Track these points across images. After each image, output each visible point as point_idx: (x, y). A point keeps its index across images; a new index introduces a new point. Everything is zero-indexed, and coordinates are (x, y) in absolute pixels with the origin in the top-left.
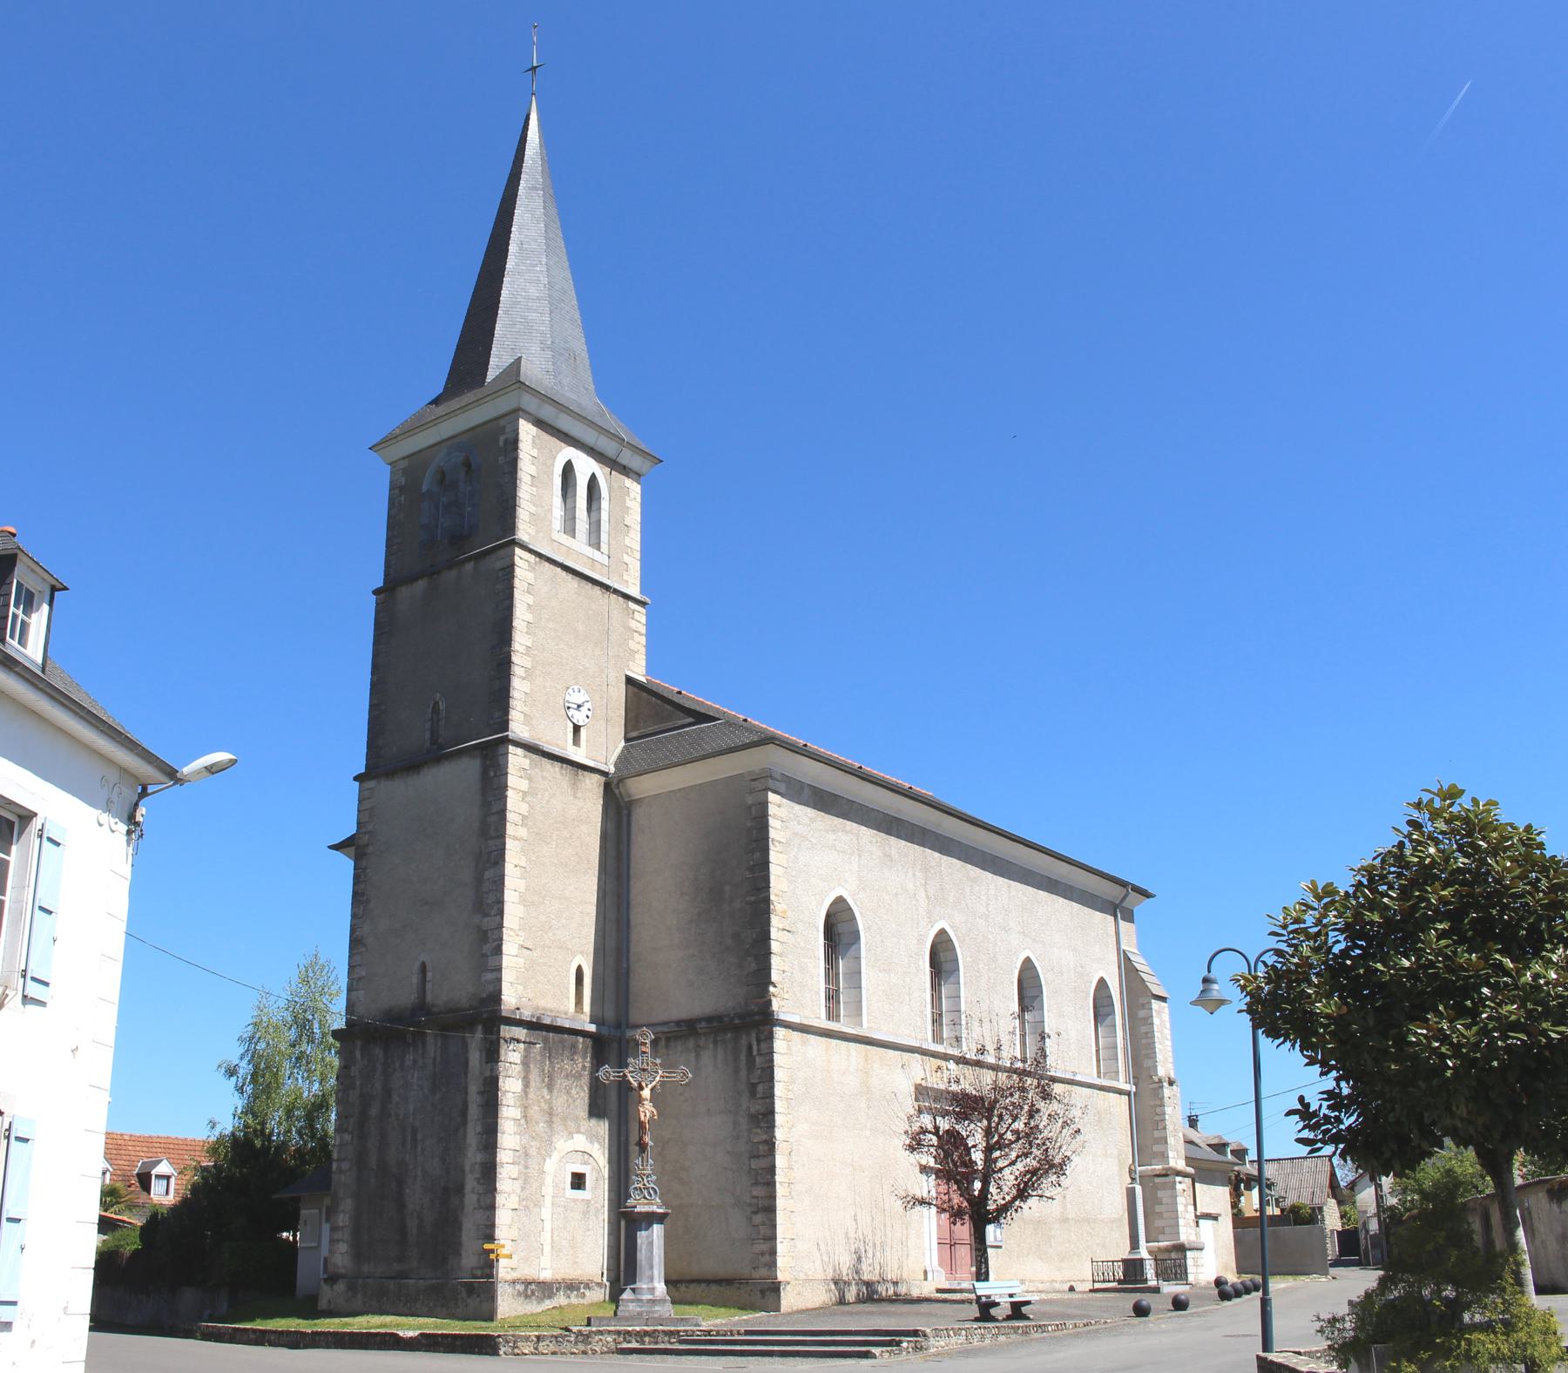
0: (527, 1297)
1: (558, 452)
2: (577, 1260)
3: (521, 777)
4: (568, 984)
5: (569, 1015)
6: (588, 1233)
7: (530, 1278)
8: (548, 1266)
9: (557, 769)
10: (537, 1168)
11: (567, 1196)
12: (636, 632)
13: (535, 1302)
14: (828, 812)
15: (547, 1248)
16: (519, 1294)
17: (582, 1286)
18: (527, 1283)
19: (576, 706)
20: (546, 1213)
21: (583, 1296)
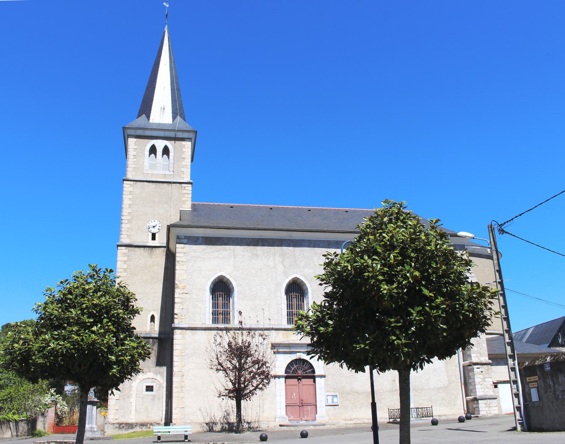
0: (120, 428)
1: (147, 144)
2: (149, 415)
3: (124, 256)
4: (147, 322)
5: (147, 332)
6: (154, 406)
7: (121, 422)
8: (134, 418)
9: (142, 250)
10: (129, 385)
11: (143, 394)
12: (186, 194)
13: (124, 430)
14: (215, 245)
15: (133, 412)
16: (116, 427)
17: (148, 425)
18: (120, 424)
19: (152, 227)
20: (133, 400)
21: (149, 428)
